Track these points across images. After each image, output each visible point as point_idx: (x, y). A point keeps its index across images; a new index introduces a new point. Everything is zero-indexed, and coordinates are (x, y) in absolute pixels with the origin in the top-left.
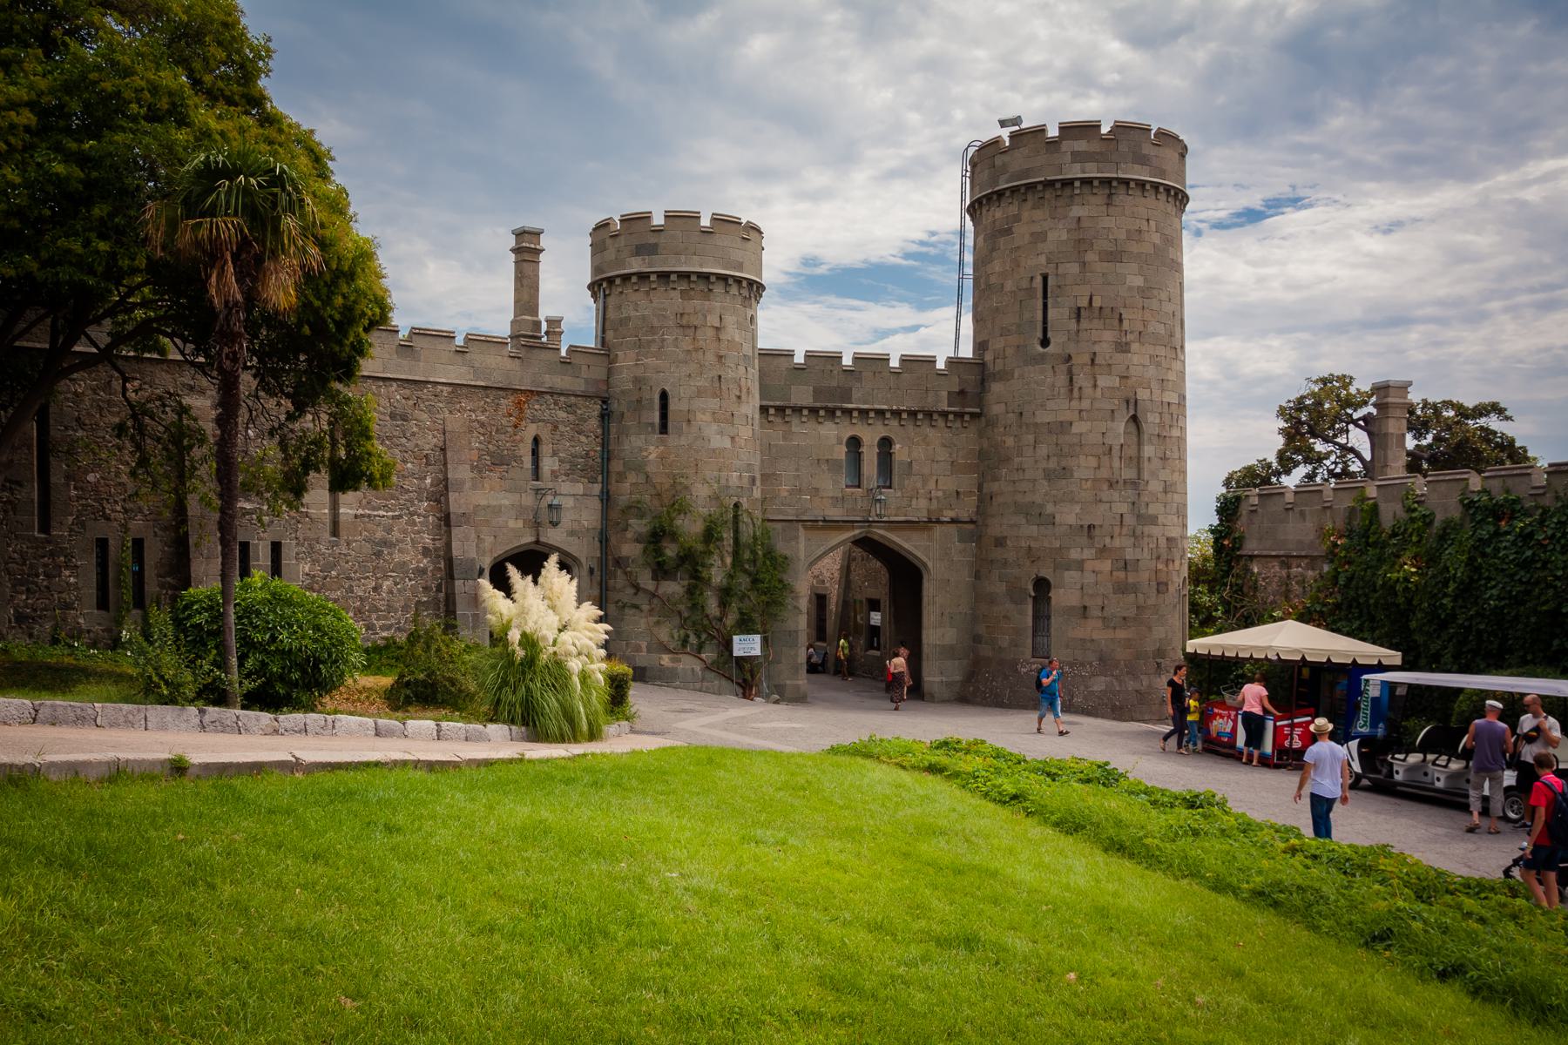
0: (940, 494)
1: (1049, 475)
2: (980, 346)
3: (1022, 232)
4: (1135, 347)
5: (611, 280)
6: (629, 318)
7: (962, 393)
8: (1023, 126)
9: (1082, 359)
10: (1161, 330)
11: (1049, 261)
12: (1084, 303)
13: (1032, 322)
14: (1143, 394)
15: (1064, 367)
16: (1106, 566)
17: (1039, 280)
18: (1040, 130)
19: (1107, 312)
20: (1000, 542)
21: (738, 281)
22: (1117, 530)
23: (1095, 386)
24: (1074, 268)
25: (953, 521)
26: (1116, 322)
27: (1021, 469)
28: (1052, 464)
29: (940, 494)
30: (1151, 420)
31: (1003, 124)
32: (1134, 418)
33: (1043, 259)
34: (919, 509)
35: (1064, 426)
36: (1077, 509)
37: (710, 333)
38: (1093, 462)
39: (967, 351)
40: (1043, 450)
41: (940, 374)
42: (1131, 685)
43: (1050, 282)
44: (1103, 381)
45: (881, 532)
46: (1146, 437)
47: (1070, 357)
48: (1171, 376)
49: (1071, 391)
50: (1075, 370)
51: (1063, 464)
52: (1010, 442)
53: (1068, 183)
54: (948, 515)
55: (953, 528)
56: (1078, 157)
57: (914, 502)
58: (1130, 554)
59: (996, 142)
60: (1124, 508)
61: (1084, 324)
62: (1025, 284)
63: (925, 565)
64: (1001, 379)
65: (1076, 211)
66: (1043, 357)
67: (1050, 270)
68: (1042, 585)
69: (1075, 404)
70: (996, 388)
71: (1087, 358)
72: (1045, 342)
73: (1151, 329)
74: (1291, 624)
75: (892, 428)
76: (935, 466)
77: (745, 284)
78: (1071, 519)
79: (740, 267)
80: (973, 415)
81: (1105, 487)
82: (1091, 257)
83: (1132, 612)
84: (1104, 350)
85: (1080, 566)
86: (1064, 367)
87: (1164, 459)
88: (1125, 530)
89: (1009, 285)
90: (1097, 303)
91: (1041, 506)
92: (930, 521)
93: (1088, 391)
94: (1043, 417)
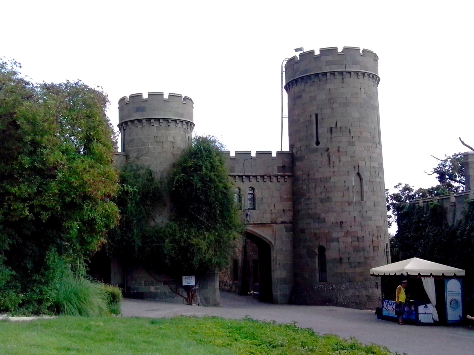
0: (276, 211)
1: (322, 201)
2: (291, 146)
3: (306, 96)
4: (357, 143)
5: (126, 123)
6: (133, 139)
7: (284, 167)
8: (305, 51)
9: (333, 150)
10: (368, 135)
11: (318, 109)
12: (333, 125)
13: (311, 134)
14: (362, 164)
15: (326, 154)
16: (349, 240)
17: (314, 117)
18: (312, 52)
19: (343, 129)
20: (303, 231)
21: (182, 121)
22: (353, 223)
23: (340, 161)
24: (328, 111)
25: (282, 223)
26: (348, 133)
27: (310, 199)
28: (323, 196)
29: (276, 211)
30: (366, 176)
31: (296, 50)
32: (358, 174)
33: (315, 108)
34: (267, 218)
35: (327, 179)
36: (335, 215)
37: (170, 144)
38: (341, 194)
39: (286, 148)
40: (318, 190)
41: (274, 159)
42: (364, 293)
43: (319, 117)
44: (343, 159)
45: (250, 228)
46: (364, 182)
47: (328, 149)
48: (375, 155)
49: (330, 163)
50: (331, 154)
51: (328, 195)
52: (305, 187)
53: (325, 74)
54: (280, 220)
55: (282, 225)
56: (329, 63)
57: (265, 215)
58: (360, 234)
59: (294, 58)
60: (356, 214)
62: (308, 118)
63: (271, 243)
64: (299, 160)
65: (329, 86)
66: (317, 150)
67: (319, 112)
68: (322, 250)
69: (331, 169)
70: (298, 164)
72: (318, 143)
73: (364, 135)
74: (415, 259)
77: (184, 123)
78: (333, 220)
79: (182, 117)
80: (289, 176)
81: (347, 204)
82: (335, 106)
83: (362, 260)
85: (337, 240)
86: (326, 154)
87: (373, 191)
88: (357, 223)
89: (302, 120)
90: (339, 125)
91: (319, 214)
92: (272, 223)
93: (337, 163)
94: (318, 176)
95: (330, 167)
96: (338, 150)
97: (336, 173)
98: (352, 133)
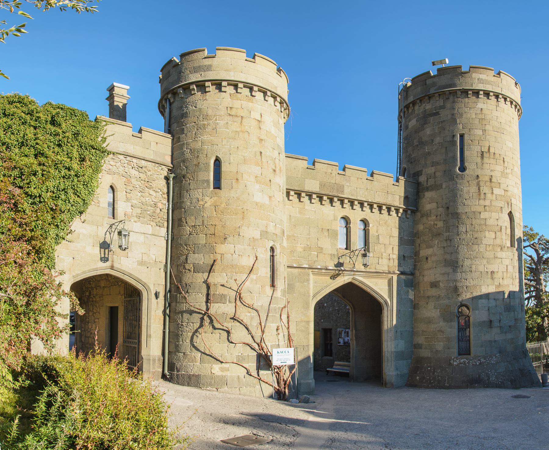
19: (497, 156)
23: (492, 193)
44: (496, 191)
49: (480, 195)
50: (482, 184)
61: (486, 160)
69: (482, 202)
71: (487, 179)
72: (463, 169)
75: (367, 213)
76: (391, 238)
84: (496, 175)
86: (475, 182)
90: (492, 150)
93: (489, 196)
95: (479, 199)
96: (491, 180)
97: (487, 208)
98: (506, 164)
